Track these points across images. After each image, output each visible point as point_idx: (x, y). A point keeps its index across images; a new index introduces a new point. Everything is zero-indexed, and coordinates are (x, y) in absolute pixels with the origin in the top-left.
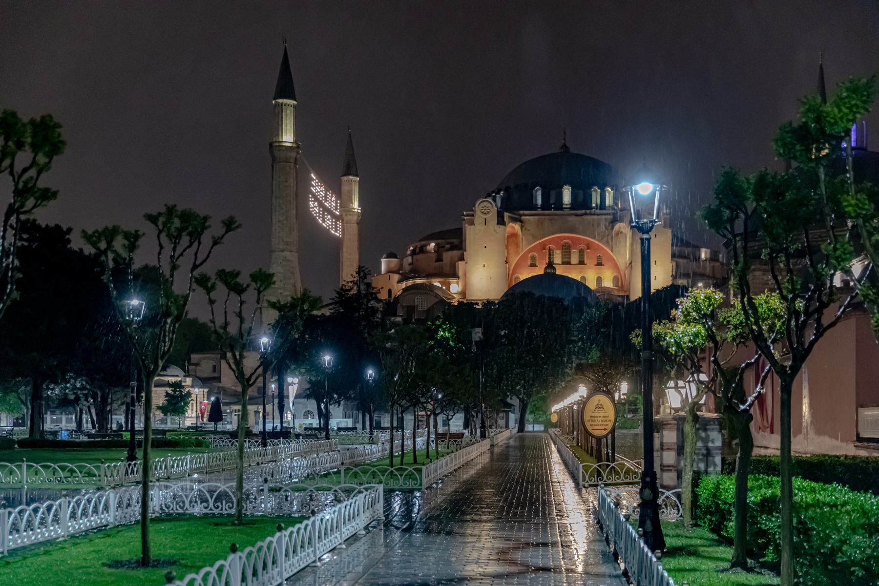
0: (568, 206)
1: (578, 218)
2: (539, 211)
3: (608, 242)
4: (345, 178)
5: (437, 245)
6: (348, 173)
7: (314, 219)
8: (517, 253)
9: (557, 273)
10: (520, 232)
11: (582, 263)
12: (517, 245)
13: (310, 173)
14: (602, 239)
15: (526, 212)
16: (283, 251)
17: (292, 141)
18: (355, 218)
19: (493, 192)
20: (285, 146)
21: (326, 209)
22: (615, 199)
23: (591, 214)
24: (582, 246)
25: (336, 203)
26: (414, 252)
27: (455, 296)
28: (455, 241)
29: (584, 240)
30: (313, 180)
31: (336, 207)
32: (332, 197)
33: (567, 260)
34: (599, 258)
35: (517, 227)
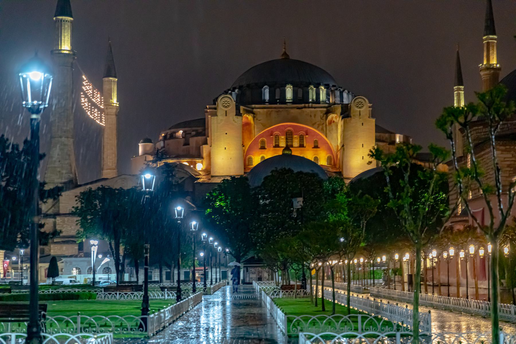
0: (291, 101)
2: (267, 105)
3: (322, 129)
4: (106, 79)
5: (184, 132)
6: (109, 75)
7: (84, 112)
8: (250, 138)
9: (293, 154)
10: (252, 122)
12: (250, 132)
13: (82, 75)
14: (318, 127)
15: (257, 106)
17: (69, 49)
18: (114, 111)
19: (229, 90)
21: (94, 105)
22: (328, 95)
23: (309, 107)
24: (302, 133)
25: (101, 99)
26: (165, 138)
27: (200, 172)
28: (200, 129)
29: (303, 128)
30: (85, 81)
31: (101, 101)
32: (97, 94)
34: (316, 142)
35: (250, 117)
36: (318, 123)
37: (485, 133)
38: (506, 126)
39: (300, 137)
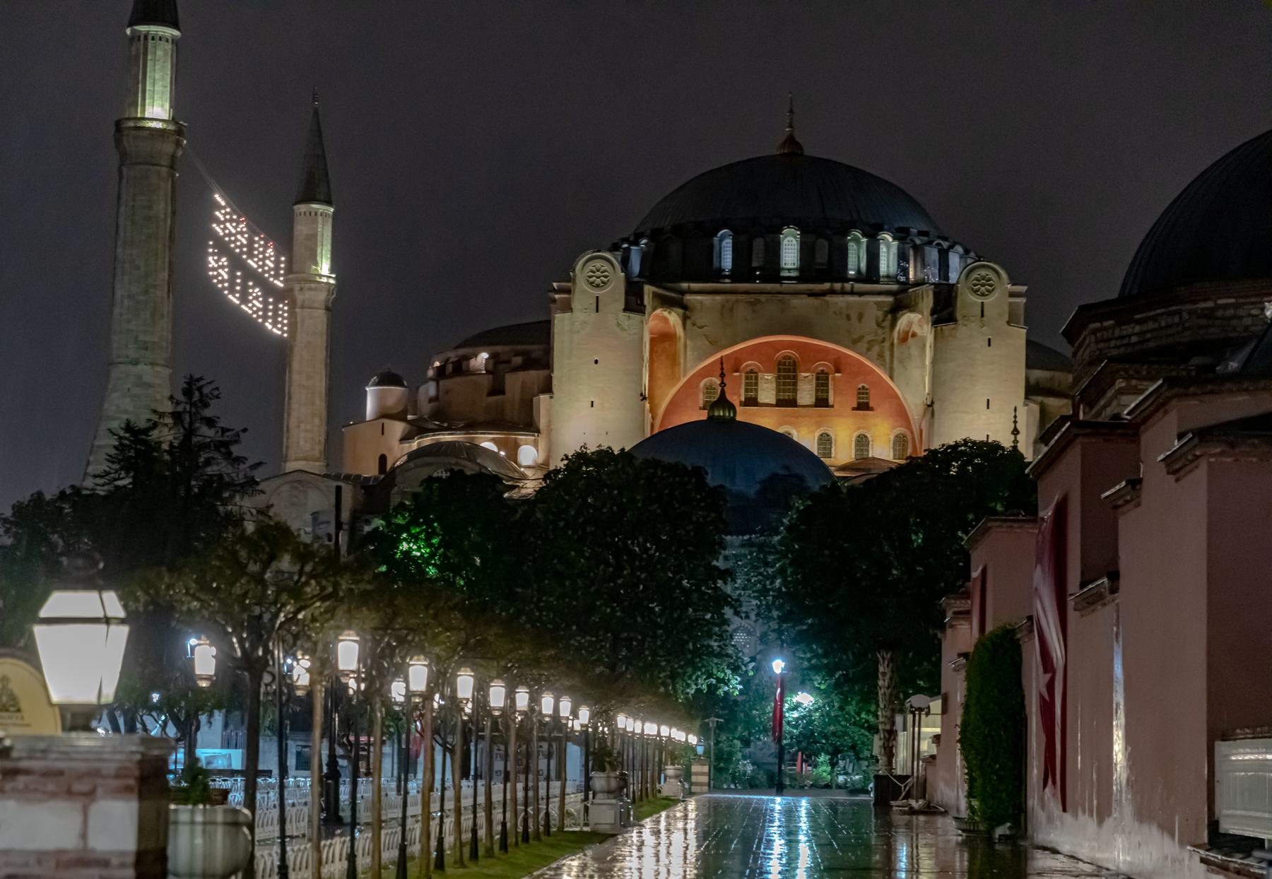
0: (794, 274)
1: (812, 301)
2: (727, 285)
3: (881, 356)
4: (302, 208)
5: (493, 356)
6: (308, 198)
7: (214, 298)
8: (674, 378)
9: (738, 418)
10: (680, 331)
11: (822, 402)
12: (674, 361)
13: (213, 192)
14: (869, 350)
15: (694, 286)
16: (135, 363)
17: (166, 117)
18: (322, 296)
19: (625, 240)
20: (150, 129)
21: (250, 274)
22: (902, 257)
23: (843, 293)
24: (822, 365)
25: (277, 262)
26: (441, 373)
27: (529, 473)
28: (536, 349)
29: (827, 350)
30: (219, 207)
31: (277, 269)
32: (266, 247)
33: (786, 396)
34: (863, 392)
35: (673, 318)
36: (868, 338)
37: (1119, 343)
38: (1177, 319)
39: (818, 379)
